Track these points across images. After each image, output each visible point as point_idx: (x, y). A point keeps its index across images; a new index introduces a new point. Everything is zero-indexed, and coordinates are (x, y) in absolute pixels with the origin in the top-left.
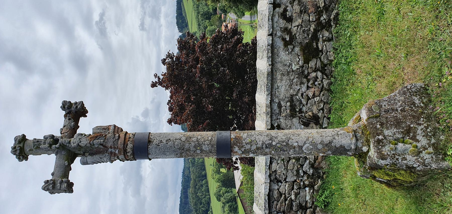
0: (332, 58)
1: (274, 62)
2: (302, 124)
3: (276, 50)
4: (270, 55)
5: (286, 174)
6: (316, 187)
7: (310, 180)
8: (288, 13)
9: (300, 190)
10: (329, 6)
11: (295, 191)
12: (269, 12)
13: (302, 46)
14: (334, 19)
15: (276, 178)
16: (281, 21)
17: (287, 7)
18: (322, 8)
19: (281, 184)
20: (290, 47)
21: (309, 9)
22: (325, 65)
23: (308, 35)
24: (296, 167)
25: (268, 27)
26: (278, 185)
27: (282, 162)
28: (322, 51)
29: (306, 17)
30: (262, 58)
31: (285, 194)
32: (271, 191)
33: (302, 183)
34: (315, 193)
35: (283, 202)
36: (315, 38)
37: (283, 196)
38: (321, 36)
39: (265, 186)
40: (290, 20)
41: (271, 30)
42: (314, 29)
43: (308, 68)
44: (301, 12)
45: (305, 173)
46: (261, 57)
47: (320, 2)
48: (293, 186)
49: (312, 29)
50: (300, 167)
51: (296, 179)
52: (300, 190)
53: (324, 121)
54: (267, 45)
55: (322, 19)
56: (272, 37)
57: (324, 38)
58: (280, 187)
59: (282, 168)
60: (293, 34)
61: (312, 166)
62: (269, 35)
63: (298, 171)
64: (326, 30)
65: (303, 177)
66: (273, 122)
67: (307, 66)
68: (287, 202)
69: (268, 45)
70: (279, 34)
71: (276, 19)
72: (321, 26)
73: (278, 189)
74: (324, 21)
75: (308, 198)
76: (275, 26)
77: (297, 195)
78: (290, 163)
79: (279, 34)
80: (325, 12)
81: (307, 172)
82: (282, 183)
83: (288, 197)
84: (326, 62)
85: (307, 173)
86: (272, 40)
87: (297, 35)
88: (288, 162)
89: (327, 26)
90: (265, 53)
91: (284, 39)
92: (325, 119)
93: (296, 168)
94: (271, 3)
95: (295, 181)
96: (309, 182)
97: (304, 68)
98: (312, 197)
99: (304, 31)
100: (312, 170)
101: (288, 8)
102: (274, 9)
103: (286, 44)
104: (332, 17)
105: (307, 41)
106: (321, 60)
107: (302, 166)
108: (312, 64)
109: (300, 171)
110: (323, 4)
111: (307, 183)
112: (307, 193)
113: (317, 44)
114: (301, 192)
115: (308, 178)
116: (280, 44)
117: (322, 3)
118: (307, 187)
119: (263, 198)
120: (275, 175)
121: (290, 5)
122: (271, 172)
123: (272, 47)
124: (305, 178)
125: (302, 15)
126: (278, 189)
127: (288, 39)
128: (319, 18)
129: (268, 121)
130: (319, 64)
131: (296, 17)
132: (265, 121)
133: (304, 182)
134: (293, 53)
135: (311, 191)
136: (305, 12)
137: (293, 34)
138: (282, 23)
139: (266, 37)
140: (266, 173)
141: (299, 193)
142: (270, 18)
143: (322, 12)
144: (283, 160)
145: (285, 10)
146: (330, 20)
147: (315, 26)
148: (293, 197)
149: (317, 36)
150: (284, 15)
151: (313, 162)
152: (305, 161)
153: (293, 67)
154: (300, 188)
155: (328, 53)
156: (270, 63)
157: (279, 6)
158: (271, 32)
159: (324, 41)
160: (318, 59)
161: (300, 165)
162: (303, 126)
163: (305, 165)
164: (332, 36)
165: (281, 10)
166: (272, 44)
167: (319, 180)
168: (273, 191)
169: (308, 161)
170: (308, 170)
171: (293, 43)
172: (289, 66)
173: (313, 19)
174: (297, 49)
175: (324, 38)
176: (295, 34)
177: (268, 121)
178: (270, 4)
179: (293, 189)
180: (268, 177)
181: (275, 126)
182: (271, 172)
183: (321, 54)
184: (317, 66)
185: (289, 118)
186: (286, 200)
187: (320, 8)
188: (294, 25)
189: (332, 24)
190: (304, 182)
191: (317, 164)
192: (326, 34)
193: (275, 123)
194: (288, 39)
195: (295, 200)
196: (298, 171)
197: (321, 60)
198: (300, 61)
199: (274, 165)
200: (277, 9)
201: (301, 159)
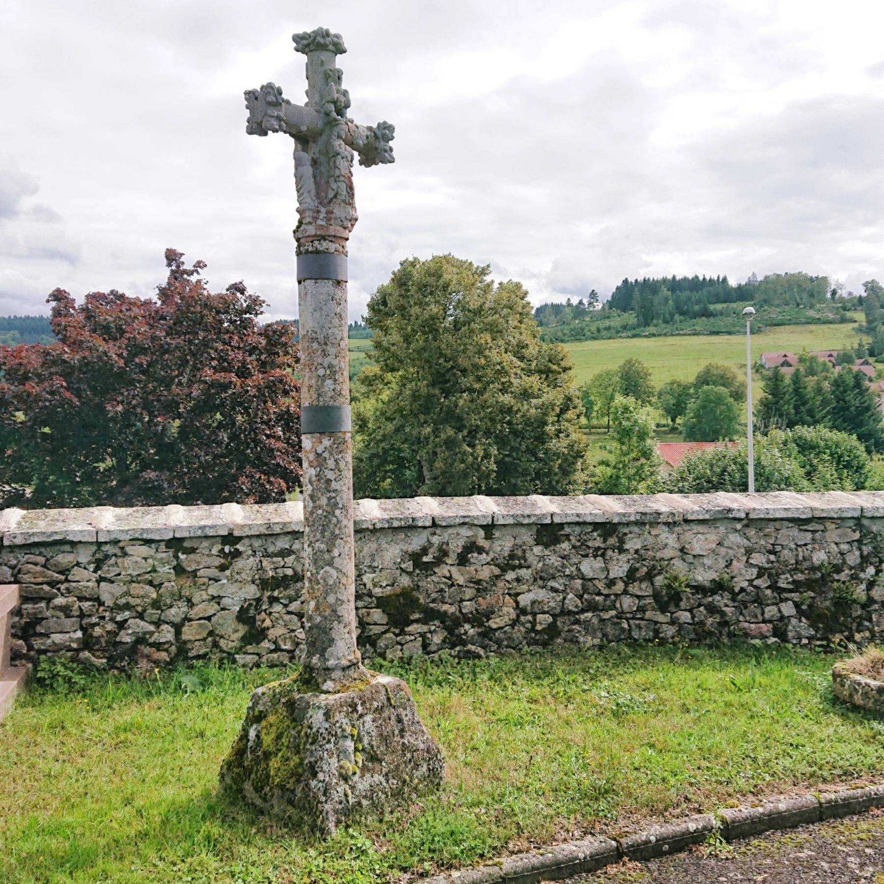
0: (389, 656)
1: (378, 534)
2: (242, 607)
3: (403, 536)
4: (396, 524)
5: (120, 580)
6: (86, 654)
7: (103, 640)
8: (475, 555)
9: (77, 617)
10: (490, 640)
11: (76, 606)
12: (477, 518)
13: (413, 590)
14: (469, 651)
15: (107, 557)
16: (461, 543)
17: (487, 554)
18: (486, 624)
19: (92, 570)
20: (409, 565)
21: (484, 598)
22: (373, 644)
23: (434, 601)
24: (138, 601)
25: (449, 517)
26: (89, 563)
27: (149, 569)
28: (402, 632)
29: (469, 593)
30: (382, 509)
31: (67, 580)
32: (72, 547)
33: (94, 620)
34: (69, 654)
35: (45, 577)
36: (429, 615)
37: (63, 577)
38: (433, 628)
39: (90, 532)
40: (463, 560)
41: (444, 524)
42: (445, 612)
43: (366, 608)
44: (478, 582)
45: (122, 625)
46: (383, 506)
47: (498, 620)
48: (87, 600)
49: (445, 607)
50: (137, 612)
51: (106, 604)
52: (77, 617)
53: (251, 656)
54: (414, 516)
55: (467, 626)
56: (429, 527)
57: (429, 635)
58: (85, 568)
59: (133, 570)
60: (436, 570)
61: (141, 640)
62: (433, 518)
63: (127, 607)
64: (445, 638)
65: (112, 620)
66: (246, 541)
67: (373, 605)
68: (46, 588)
69: (414, 519)
70: (435, 540)
71: (465, 532)
72: (451, 624)
73: (78, 564)
74: (462, 631)
75: (57, 638)
76: (450, 531)
77: (66, 610)
78: (147, 587)
79: (435, 540)
80: (480, 630)
81: (125, 629)
82: (95, 571)
83: (59, 589)
84: (381, 643)
85: (120, 631)
86: (425, 528)
87: (433, 578)
88: (150, 583)
89: (454, 640)
90: (395, 514)
91: (424, 551)
92: (256, 658)
93: (133, 601)
94: (495, 519)
95: (101, 603)
96: (98, 638)
97: (367, 599)
98: (57, 649)
99: (441, 591)
100: (129, 641)
101: (484, 554)
102: (482, 526)
103: (416, 557)
104: (470, 647)
105: (422, 601)
106: (384, 633)
107: (141, 616)
108: (377, 615)
109: (127, 613)
110: (494, 626)
111: (98, 631)
112: (68, 635)
113: (417, 621)
114: (73, 619)
115: (108, 632)
116: (416, 542)
117: (496, 623)
118: (83, 634)
119: (56, 529)
120: (115, 555)
121: (489, 559)
122: (121, 544)
123: (410, 527)
124: (110, 627)
125: (472, 585)
126: (78, 564)
127: (425, 559)
128: (467, 620)
129: (250, 529)
130: (376, 630)
131: (468, 572)
132: (250, 523)
133: (97, 624)
134: (398, 572)
135: (74, 645)
136: (478, 590)
137: (436, 570)
138: (456, 546)
139: (429, 513)
140: (122, 531)
141: (68, 616)
142: (467, 520)
143: (481, 625)
144: (154, 570)
145: (480, 550)
146: (464, 643)
147: (452, 614)
148: (60, 601)
149: (432, 620)
150: (472, 547)
151: (151, 640)
152: (151, 623)
153: (368, 575)
154: (82, 615)
155: (399, 647)
156: (378, 526)
157: (489, 536)
158: (439, 523)
159: (423, 635)
160: (386, 627)
161: (144, 611)
162: (238, 609)
163: (142, 623)
164: (434, 652)
165: (482, 542)
166: (416, 527)
167: (105, 661)
168: (72, 552)
169: (152, 628)
170: (130, 631)
171: (418, 571)
172: (370, 567)
173: (465, 607)
174: (405, 581)
175: (429, 635)
176: (435, 573)
177: (250, 529)
178: (493, 518)
179: (81, 599)
180: (112, 537)
181: (238, 546)
182: (121, 544)
183: (397, 631)
184: (371, 627)
185: (257, 577)
186: (52, 584)
187: (488, 621)
188: (454, 570)
189: (458, 649)
190: (97, 624)
191: (147, 650)
192: (437, 639)
193: (244, 545)
194: (425, 559)
195: (51, 605)
196: (127, 607)
197: (384, 633)
198: (380, 590)
199: (144, 550)
200: (482, 533)
201: (159, 612)
